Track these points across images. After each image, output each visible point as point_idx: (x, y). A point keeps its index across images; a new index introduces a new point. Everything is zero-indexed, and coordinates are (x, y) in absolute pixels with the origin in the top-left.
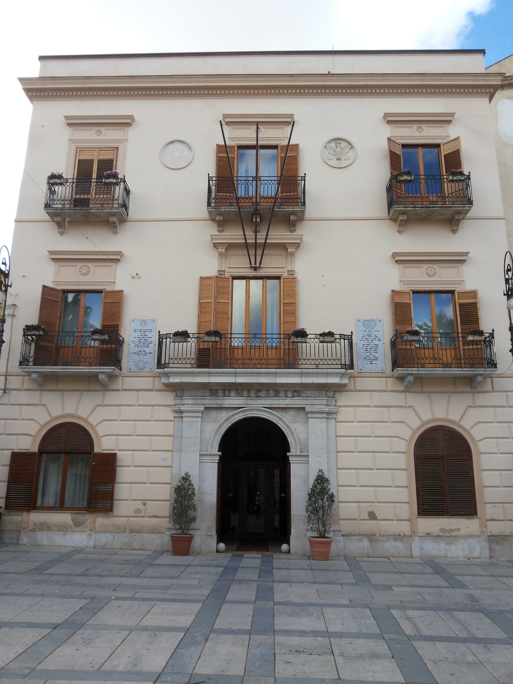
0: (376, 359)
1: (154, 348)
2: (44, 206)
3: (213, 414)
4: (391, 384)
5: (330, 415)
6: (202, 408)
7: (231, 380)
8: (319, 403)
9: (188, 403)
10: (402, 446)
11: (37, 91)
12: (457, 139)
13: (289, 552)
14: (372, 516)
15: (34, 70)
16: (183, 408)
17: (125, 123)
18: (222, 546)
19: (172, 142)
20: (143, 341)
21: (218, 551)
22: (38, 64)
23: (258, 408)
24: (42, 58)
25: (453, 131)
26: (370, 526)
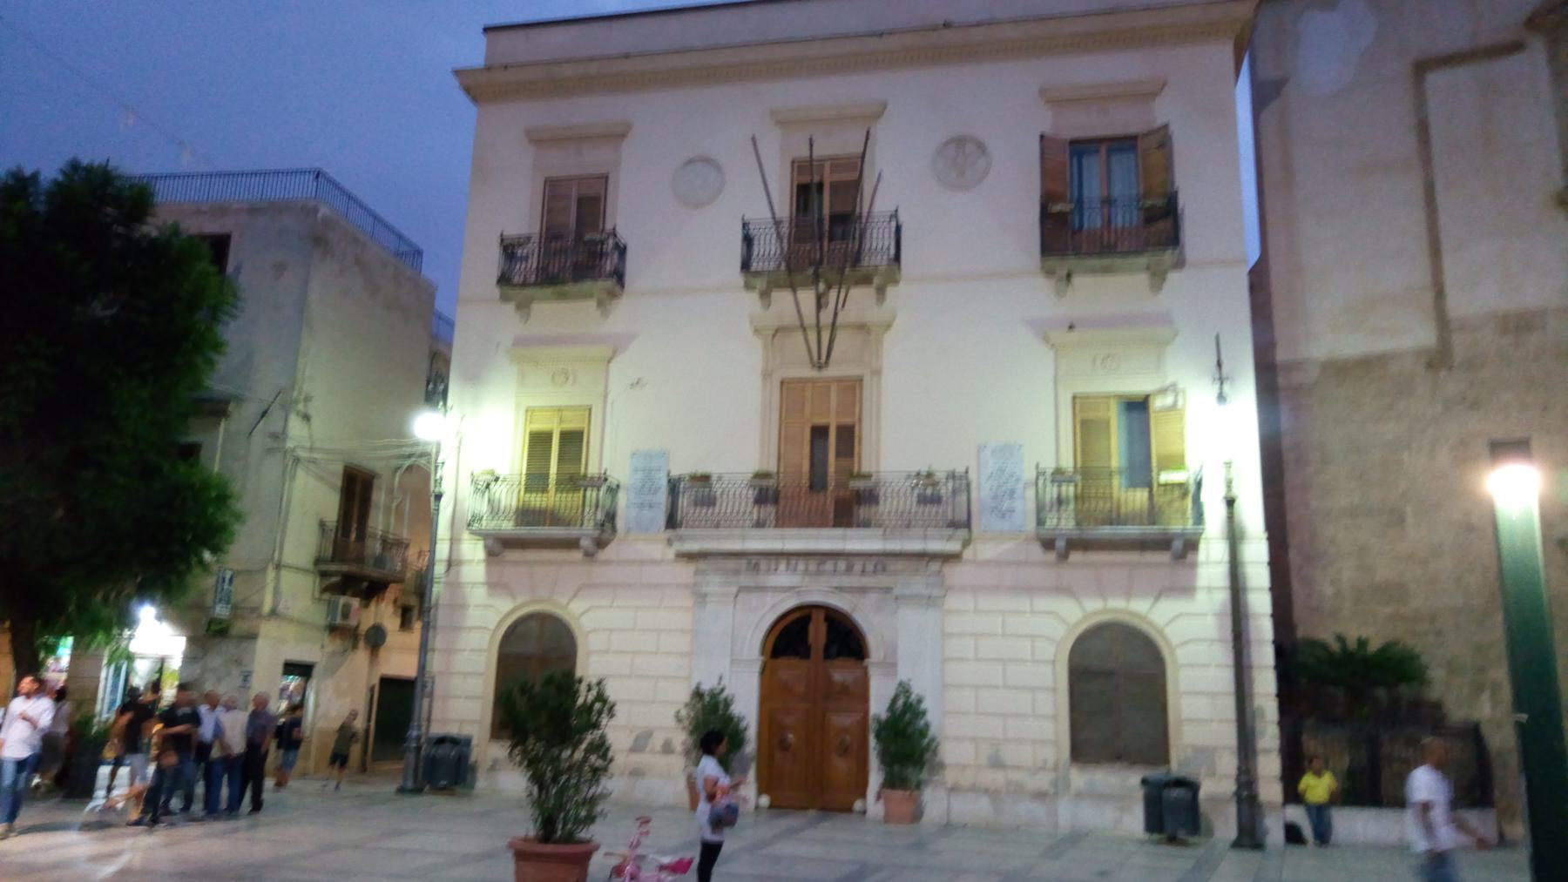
0: (1012, 511)
1: (662, 497)
2: (494, 280)
3: (754, 599)
4: (1037, 552)
5: (931, 601)
6: (734, 589)
7: (776, 545)
8: (917, 583)
9: (714, 583)
10: (1046, 650)
11: (481, 87)
12: (1166, 127)
13: (864, 812)
14: (997, 763)
15: (474, 53)
16: (705, 590)
17: (616, 136)
18: (765, 800)
19: (690, 162)
20: (646, 487)
21: (757, 807)
22: (482, 41)
23: (820, 591)
24: (487, 30)
25: (1164, 111)
26: (995, 778)
